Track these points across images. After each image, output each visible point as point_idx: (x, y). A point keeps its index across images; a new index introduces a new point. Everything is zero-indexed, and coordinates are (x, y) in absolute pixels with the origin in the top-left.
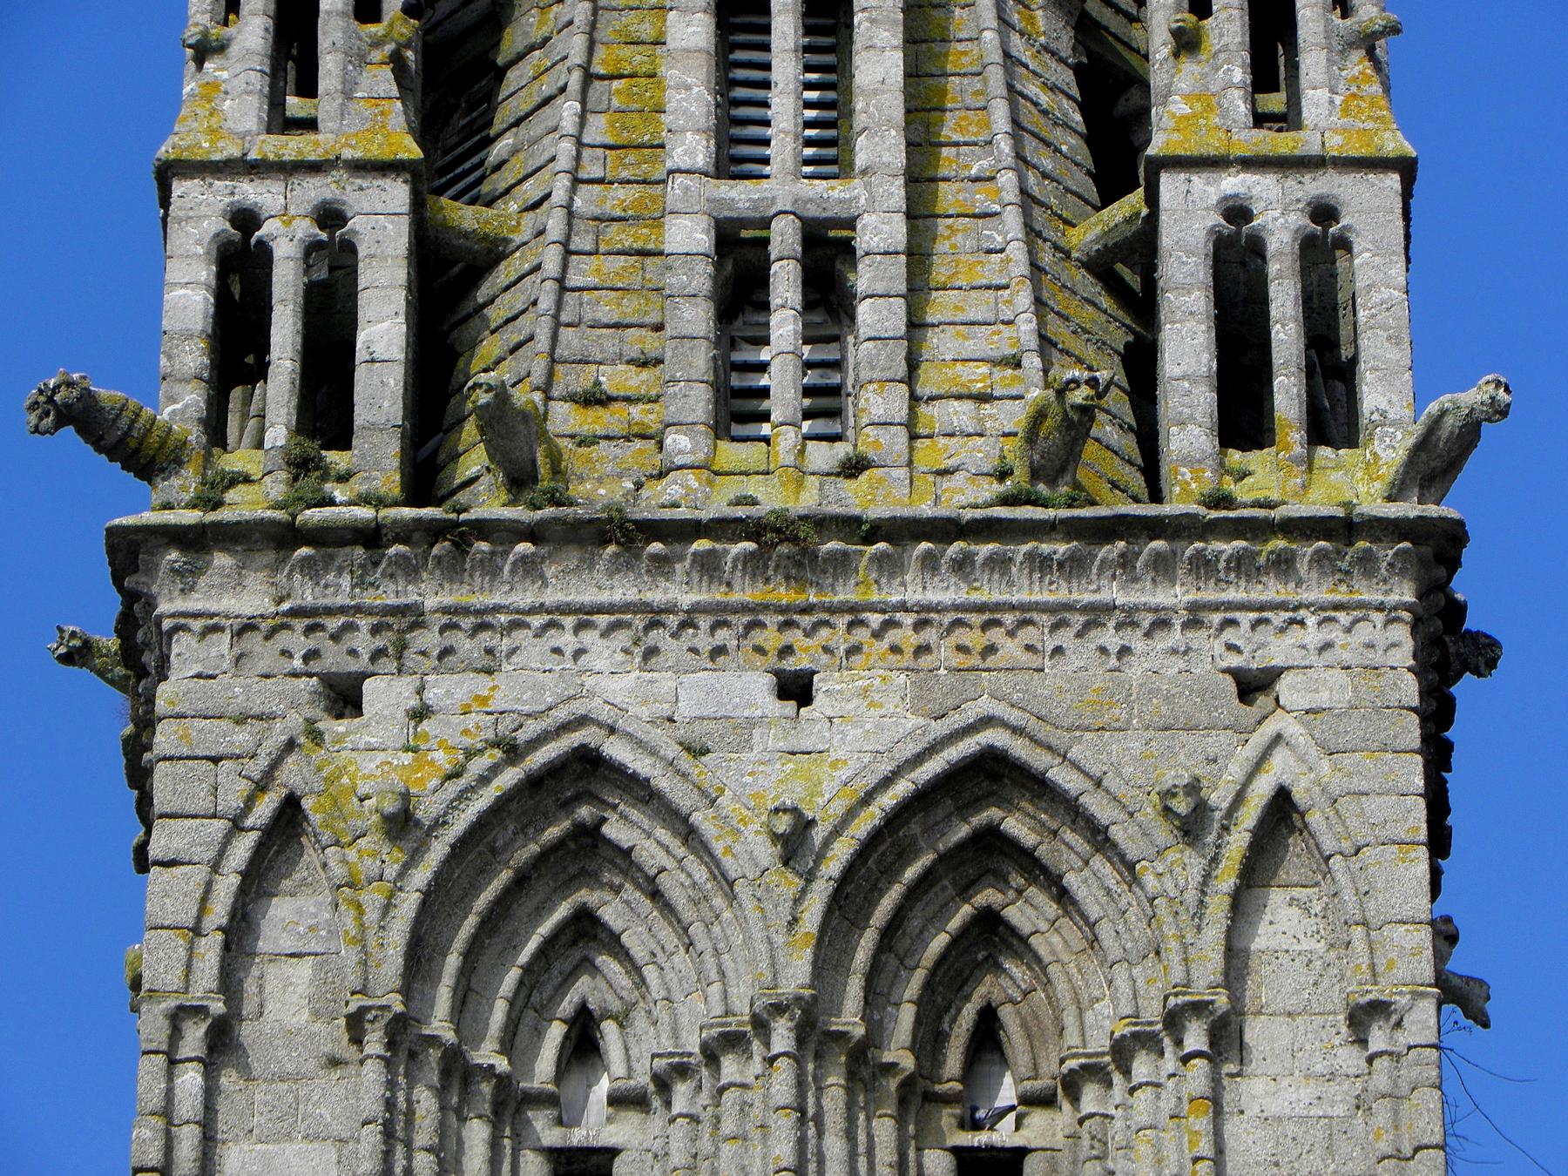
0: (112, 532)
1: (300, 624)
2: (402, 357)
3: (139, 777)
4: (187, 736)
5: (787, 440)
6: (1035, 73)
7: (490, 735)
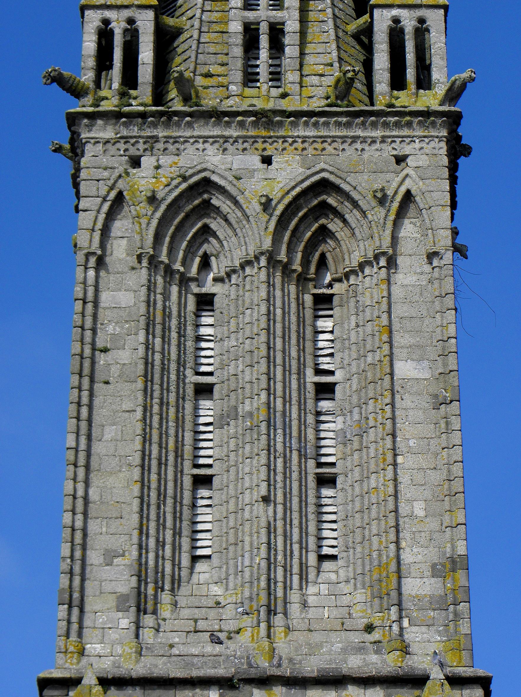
0: (68, 114)
1: (122, 141)
2: (152, 63)
3: (76, 185)
4: (89, 173)
5: (264, 87)
7: (178, 174)
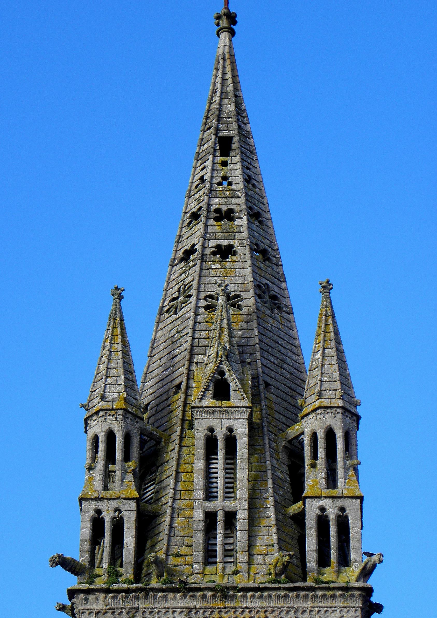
1: (111, 612)
2: (134, 546)
5: (220, 566)
6: (278, 469)
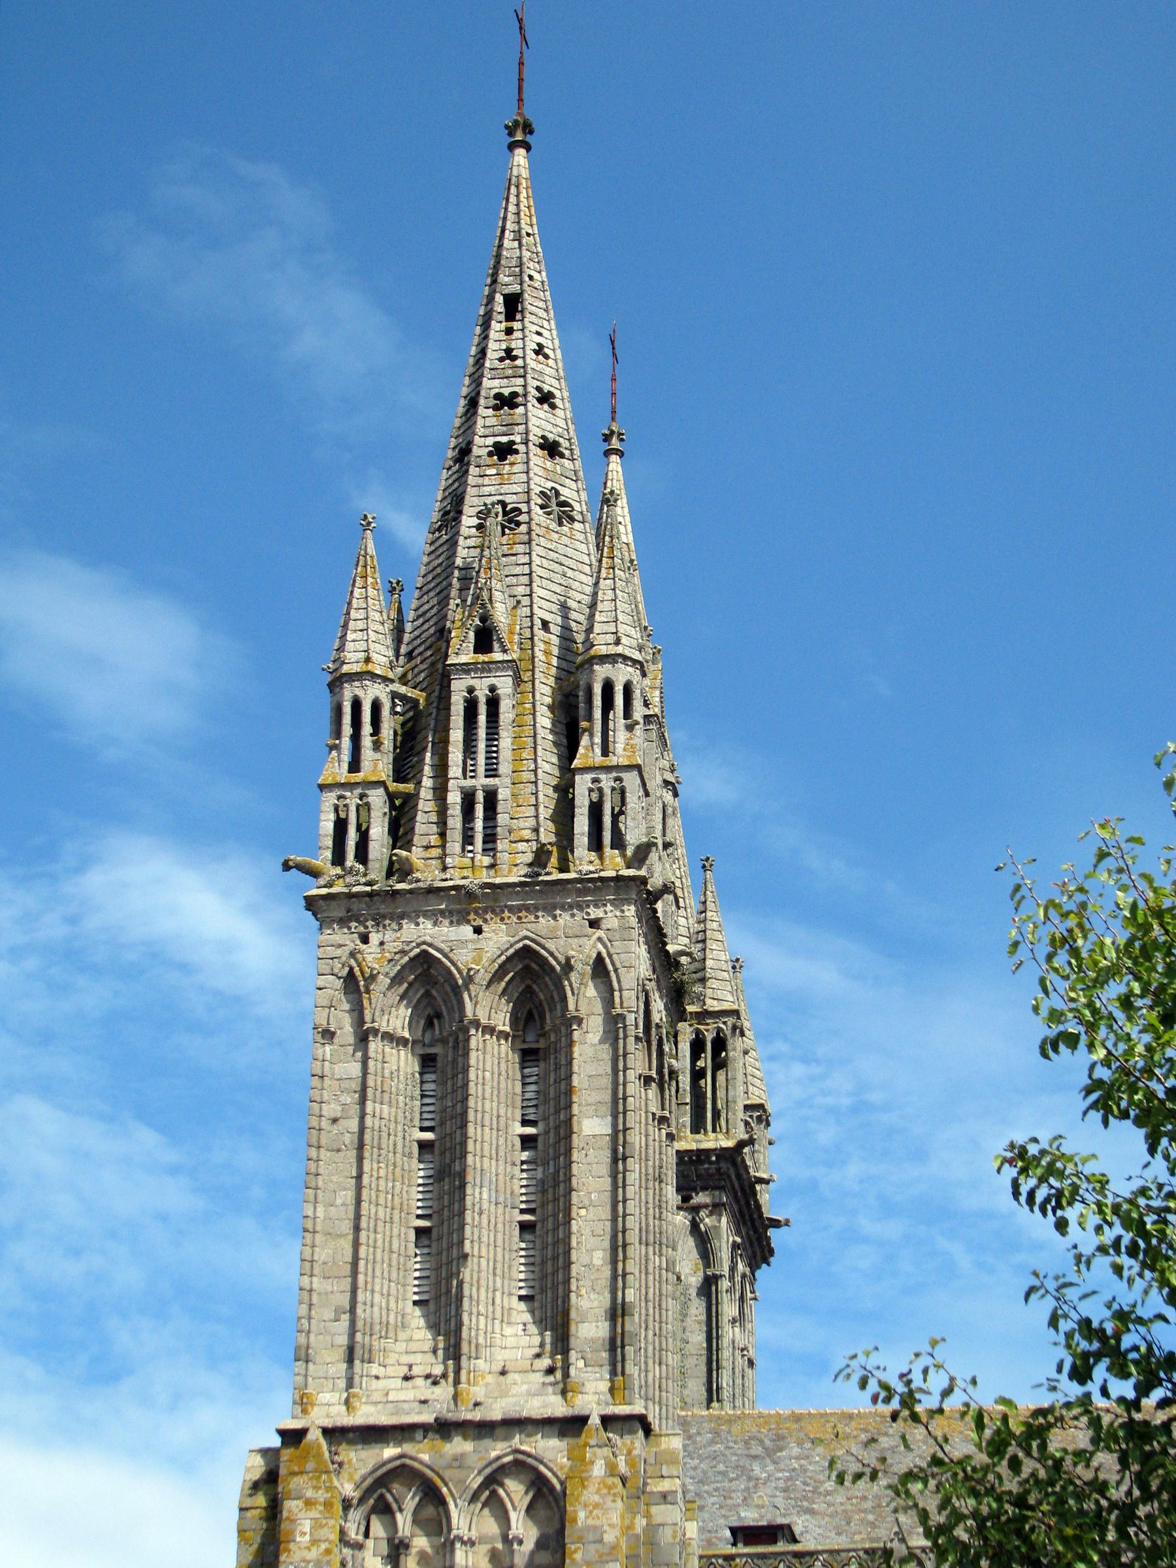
0: (306, 898)
